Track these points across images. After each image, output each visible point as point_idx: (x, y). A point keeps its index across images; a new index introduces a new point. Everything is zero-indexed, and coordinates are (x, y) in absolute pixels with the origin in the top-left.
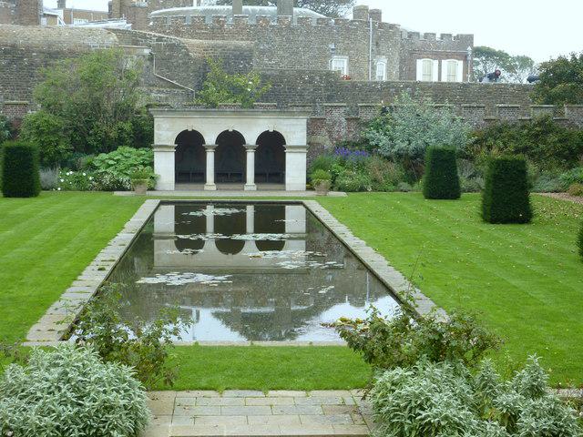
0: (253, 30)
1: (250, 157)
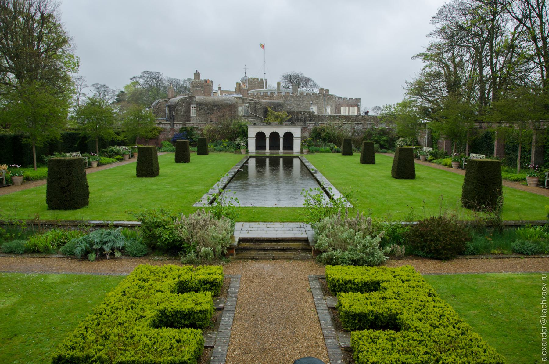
1: (281, 141)
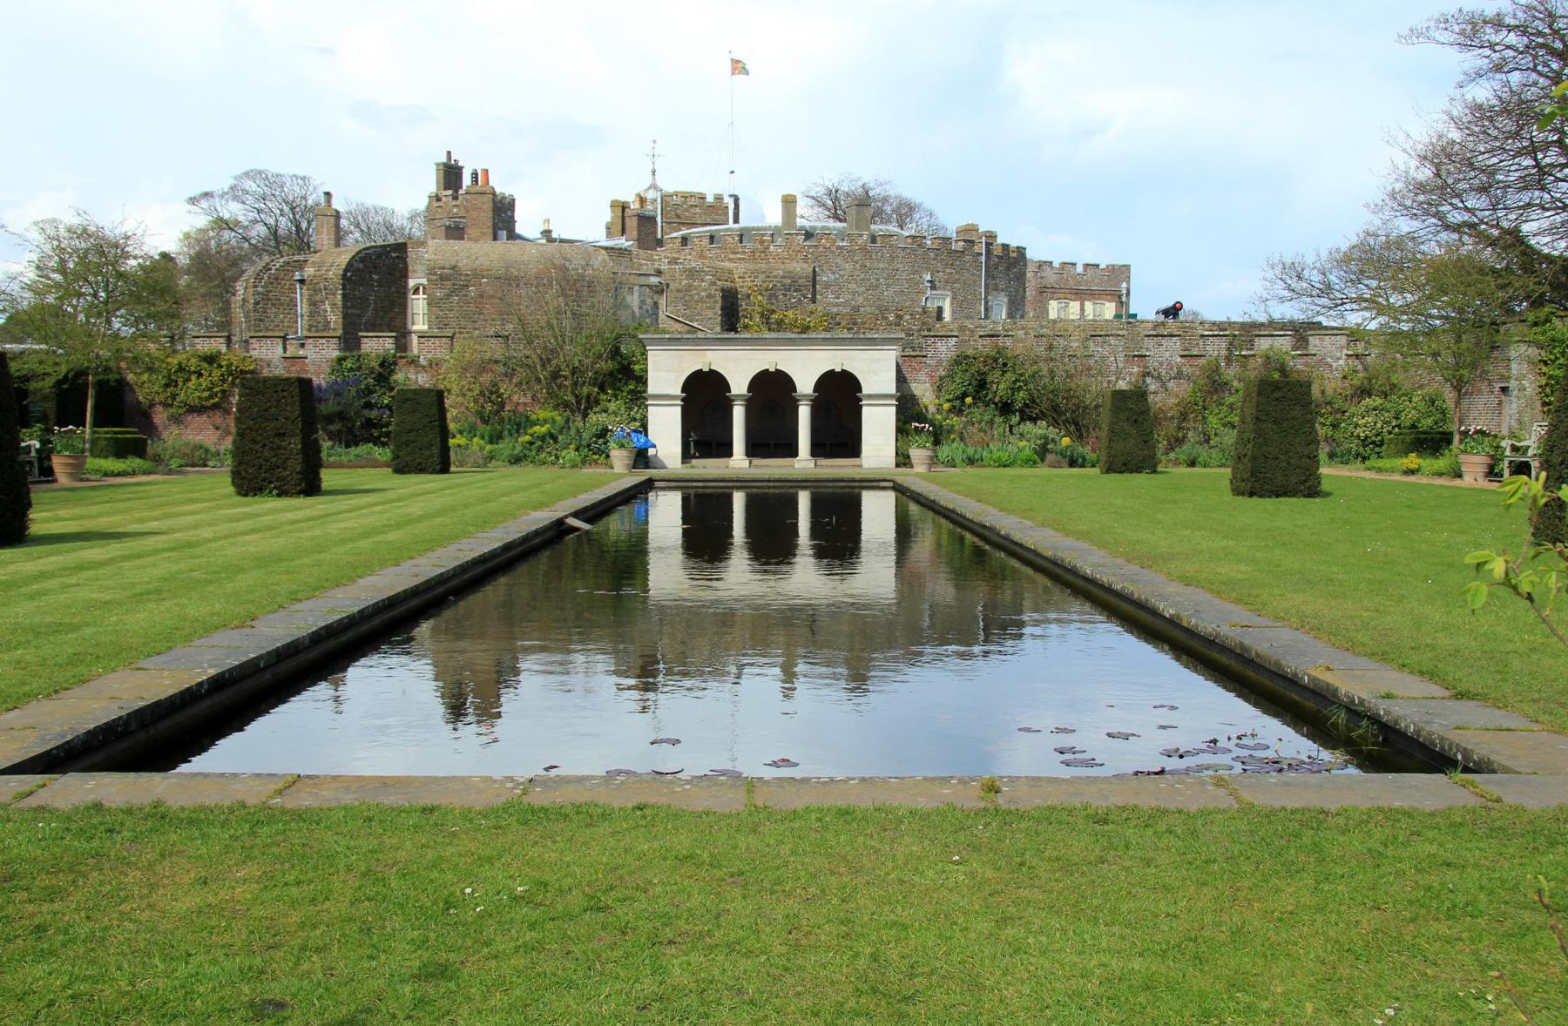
1: (804, 413)
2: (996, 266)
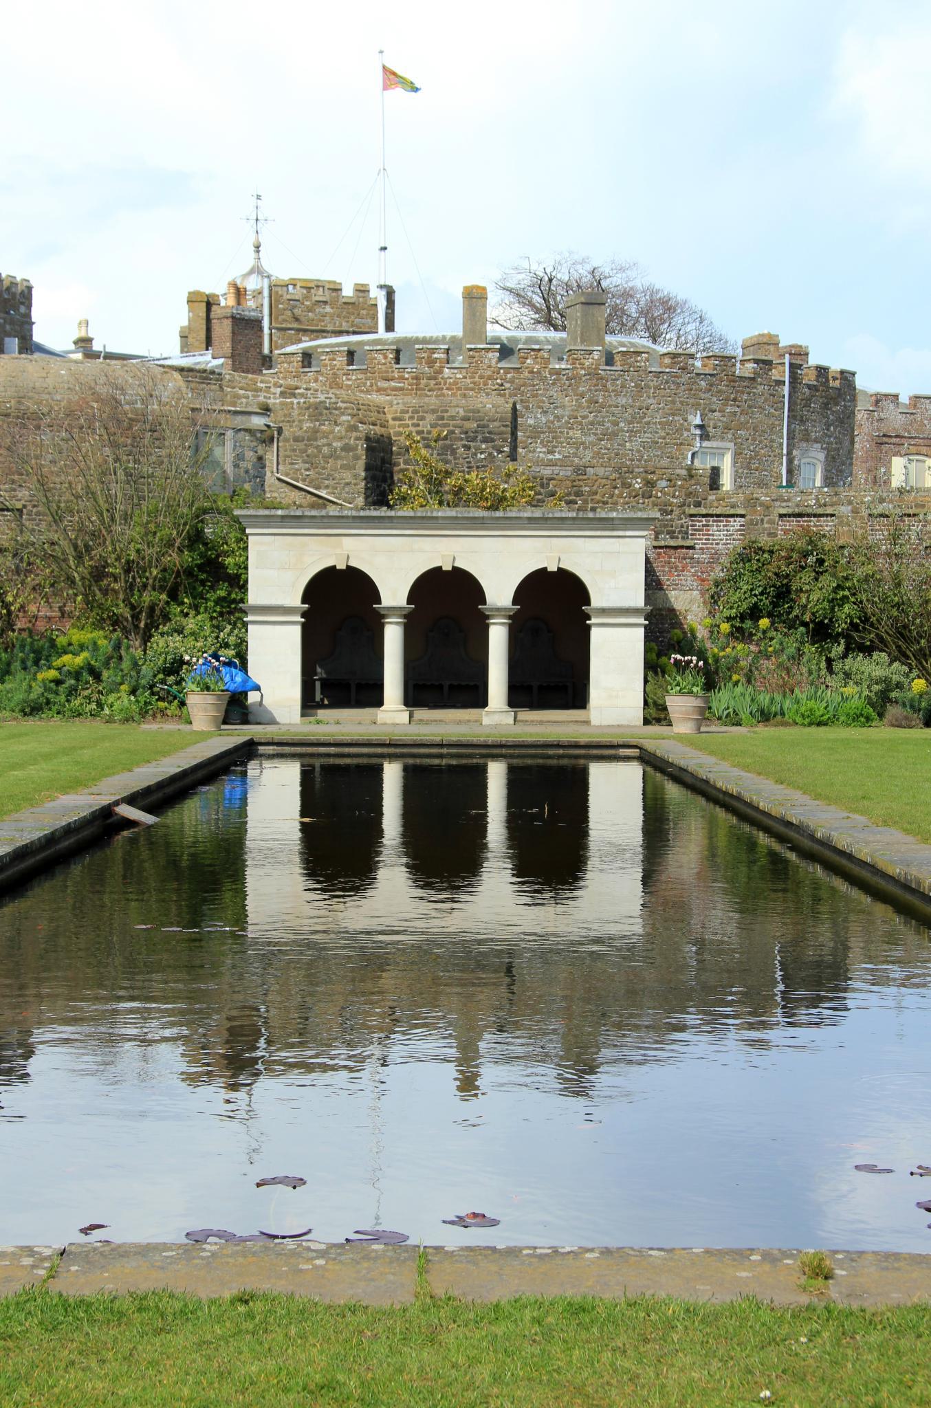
0: (511, 382)
1: (498, 637)
2: (808, 402)
